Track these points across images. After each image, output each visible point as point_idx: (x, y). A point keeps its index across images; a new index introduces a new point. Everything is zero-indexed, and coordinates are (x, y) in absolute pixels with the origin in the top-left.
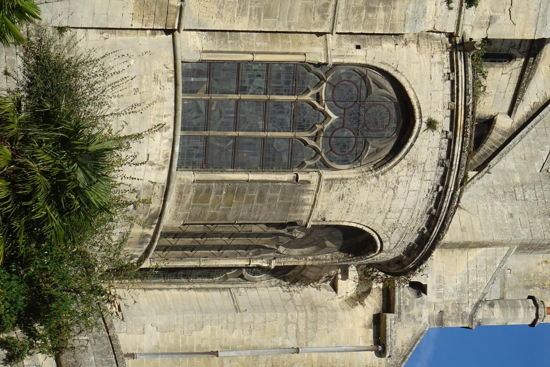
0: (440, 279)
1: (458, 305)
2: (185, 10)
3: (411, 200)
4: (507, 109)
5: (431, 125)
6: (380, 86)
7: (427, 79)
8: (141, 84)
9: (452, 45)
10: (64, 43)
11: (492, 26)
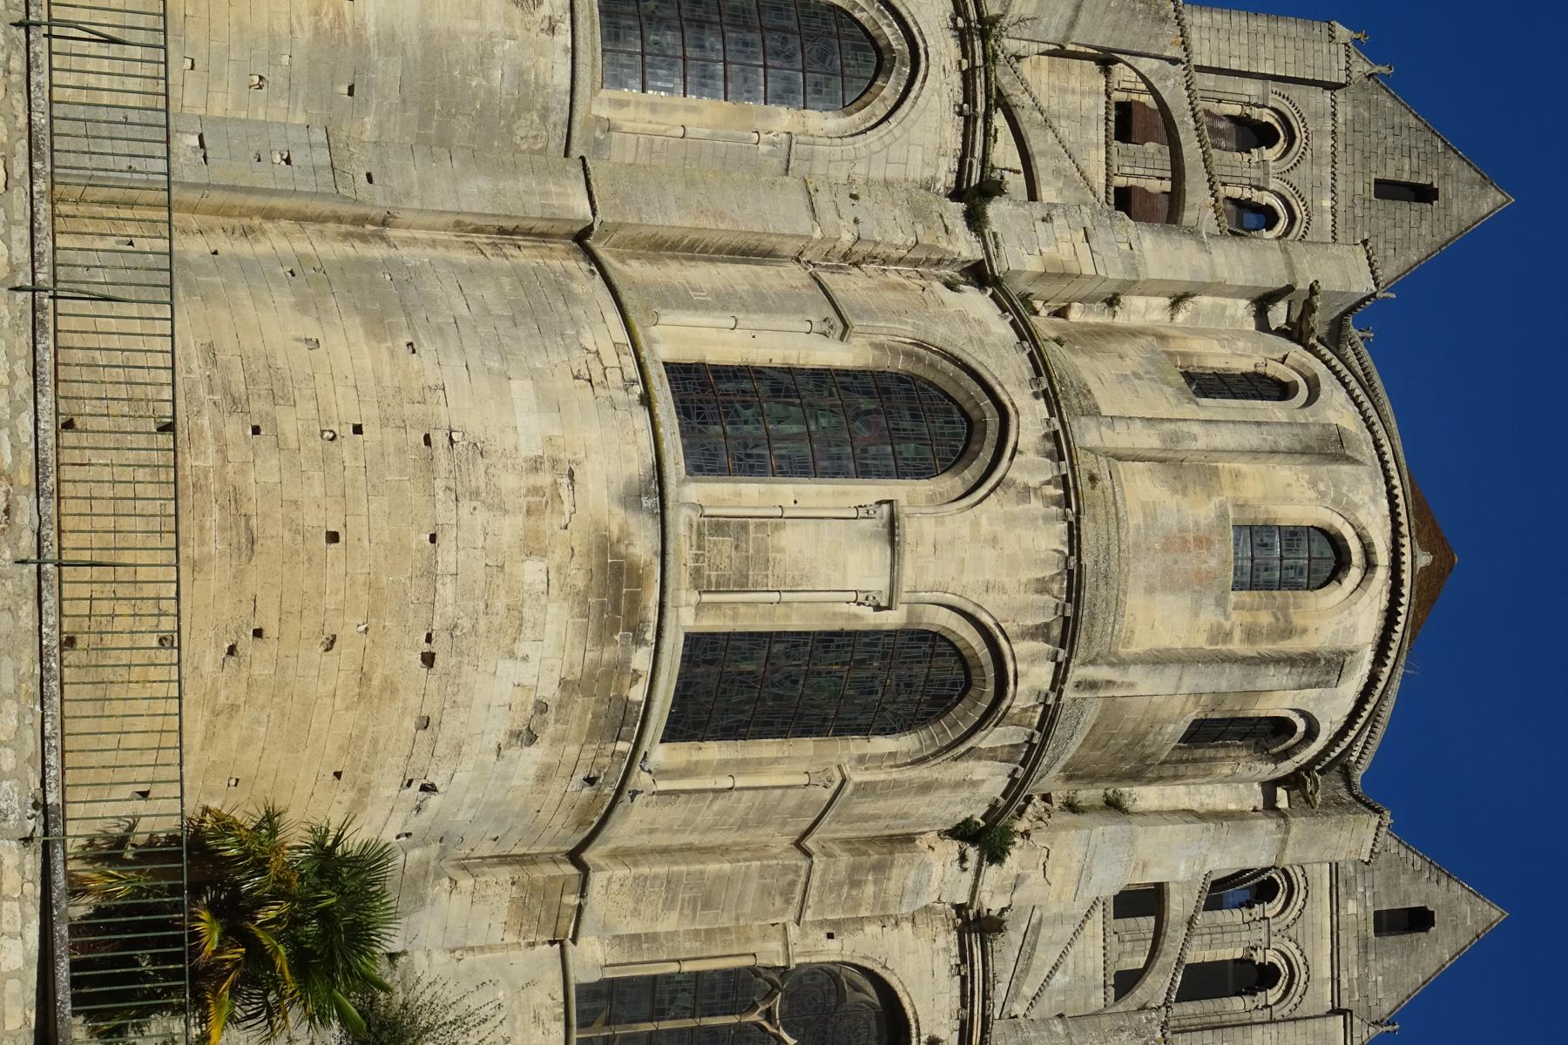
2: (587, 910)
6: (857, 988)
7: (928, 977)
8: (513, 1029)
9: (963, 923)
10: (398, 978)
11: (1018, 890)
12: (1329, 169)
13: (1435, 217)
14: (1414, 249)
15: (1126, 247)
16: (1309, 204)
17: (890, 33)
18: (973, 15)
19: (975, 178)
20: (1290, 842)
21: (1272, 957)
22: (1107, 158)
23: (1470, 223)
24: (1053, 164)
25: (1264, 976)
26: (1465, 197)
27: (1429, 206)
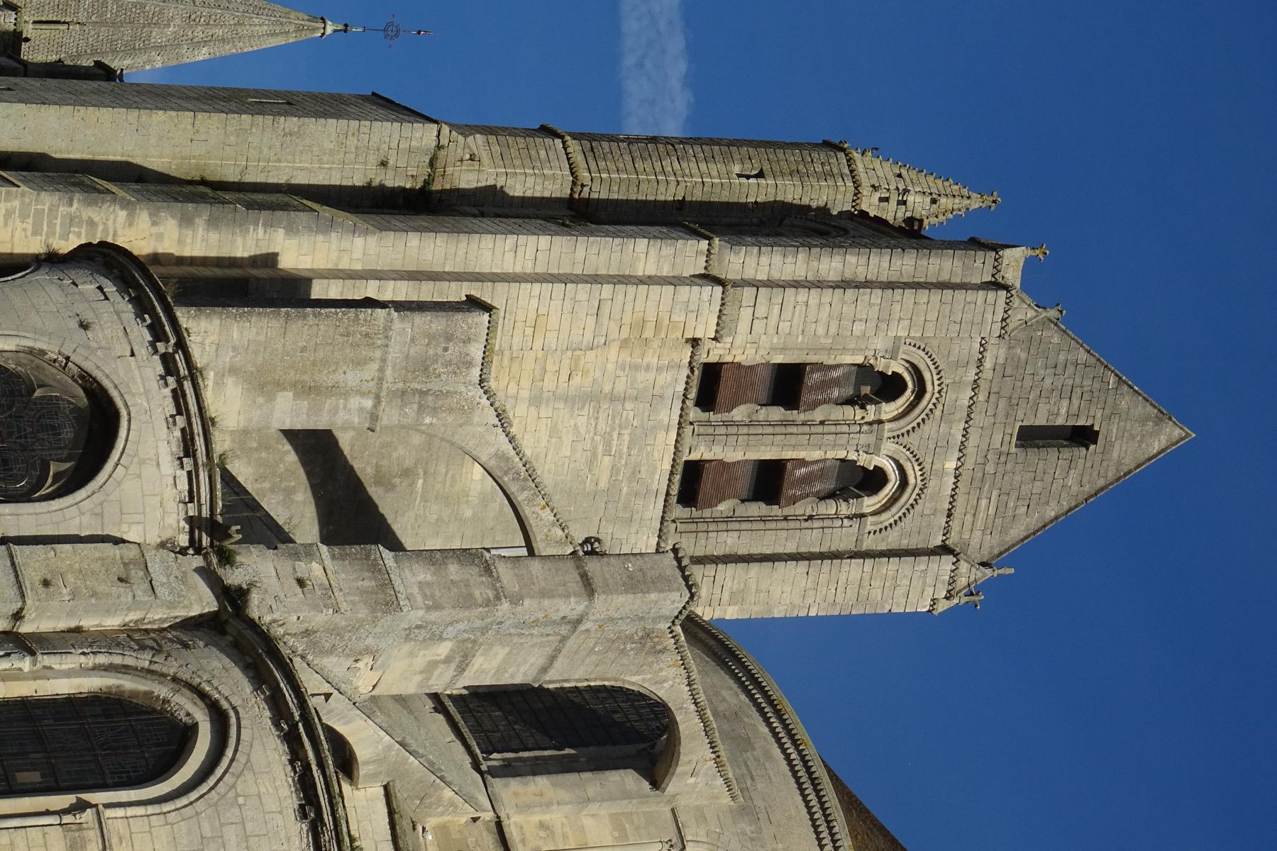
12: (962, 425)
13: (1089, 464)
14: (1053, 504)
16: (928, 467)
22: (677, 441)
23: (1133, 466)
26: (1133, 437)
27: (1083, 450)
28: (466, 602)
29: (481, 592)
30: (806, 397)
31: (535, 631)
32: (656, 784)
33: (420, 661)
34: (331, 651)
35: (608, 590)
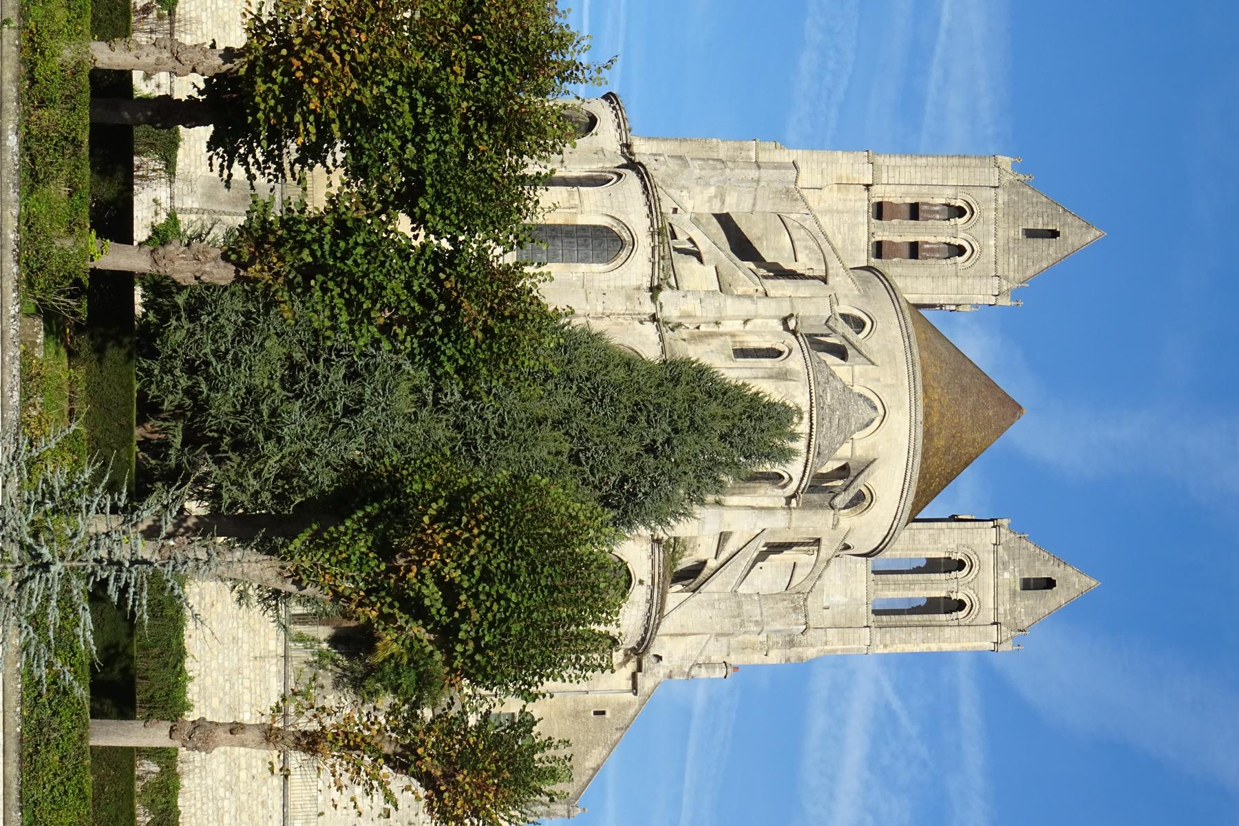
0: (670, 653)
1: (681, 667)
3: (633, 620)
4: (714, 556)
5: (641, 582)
15: (717, 304)
17: (625, 235)
18: (656, 227)
19: (656, 284)
20: (793, 519)
21: (960, 596)
24: (804, 244)
25: (961, 605)
28: (715, 168)
29: (719, 165)
30: (921, 214)
31: (744, 185)
32: (826, 283)
33: (706, 198)
34: (671, 186)
35: (766, 168)
